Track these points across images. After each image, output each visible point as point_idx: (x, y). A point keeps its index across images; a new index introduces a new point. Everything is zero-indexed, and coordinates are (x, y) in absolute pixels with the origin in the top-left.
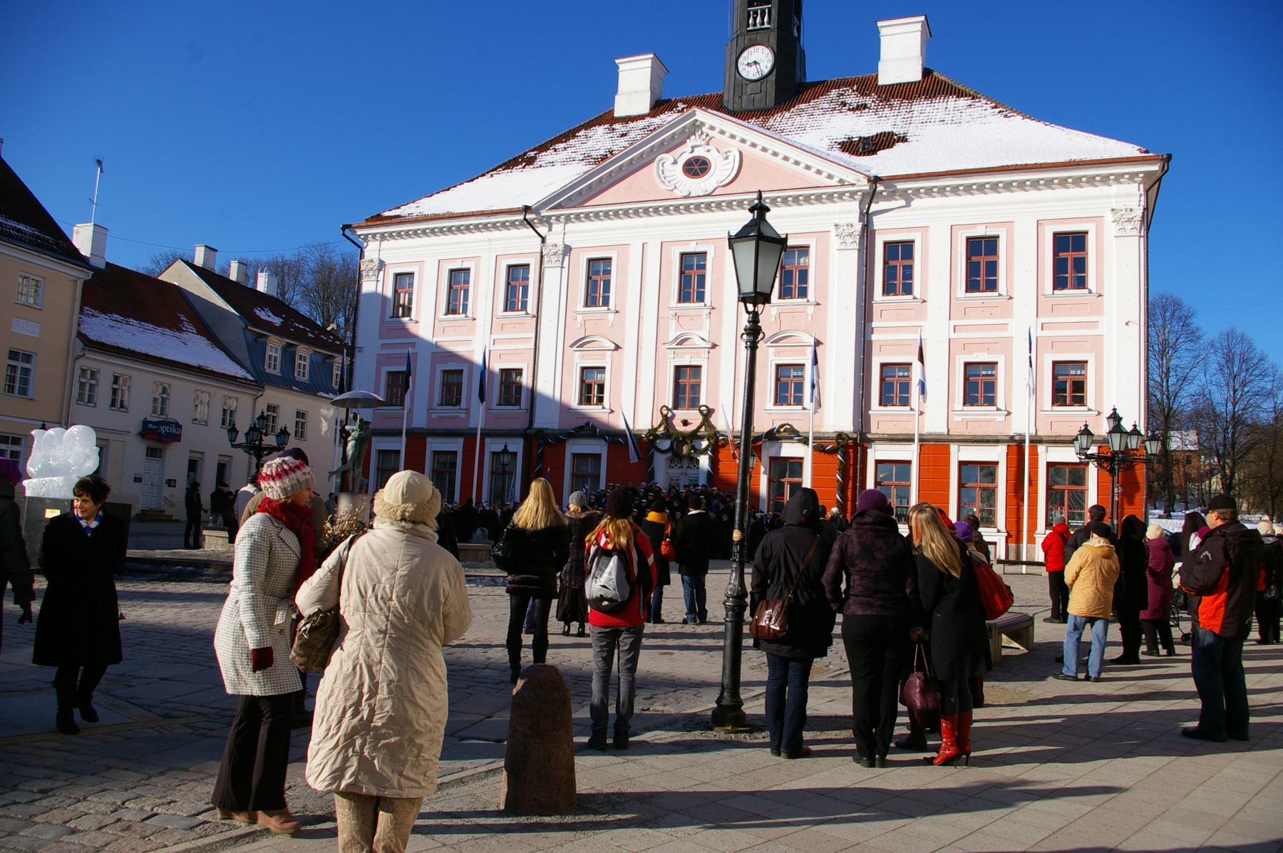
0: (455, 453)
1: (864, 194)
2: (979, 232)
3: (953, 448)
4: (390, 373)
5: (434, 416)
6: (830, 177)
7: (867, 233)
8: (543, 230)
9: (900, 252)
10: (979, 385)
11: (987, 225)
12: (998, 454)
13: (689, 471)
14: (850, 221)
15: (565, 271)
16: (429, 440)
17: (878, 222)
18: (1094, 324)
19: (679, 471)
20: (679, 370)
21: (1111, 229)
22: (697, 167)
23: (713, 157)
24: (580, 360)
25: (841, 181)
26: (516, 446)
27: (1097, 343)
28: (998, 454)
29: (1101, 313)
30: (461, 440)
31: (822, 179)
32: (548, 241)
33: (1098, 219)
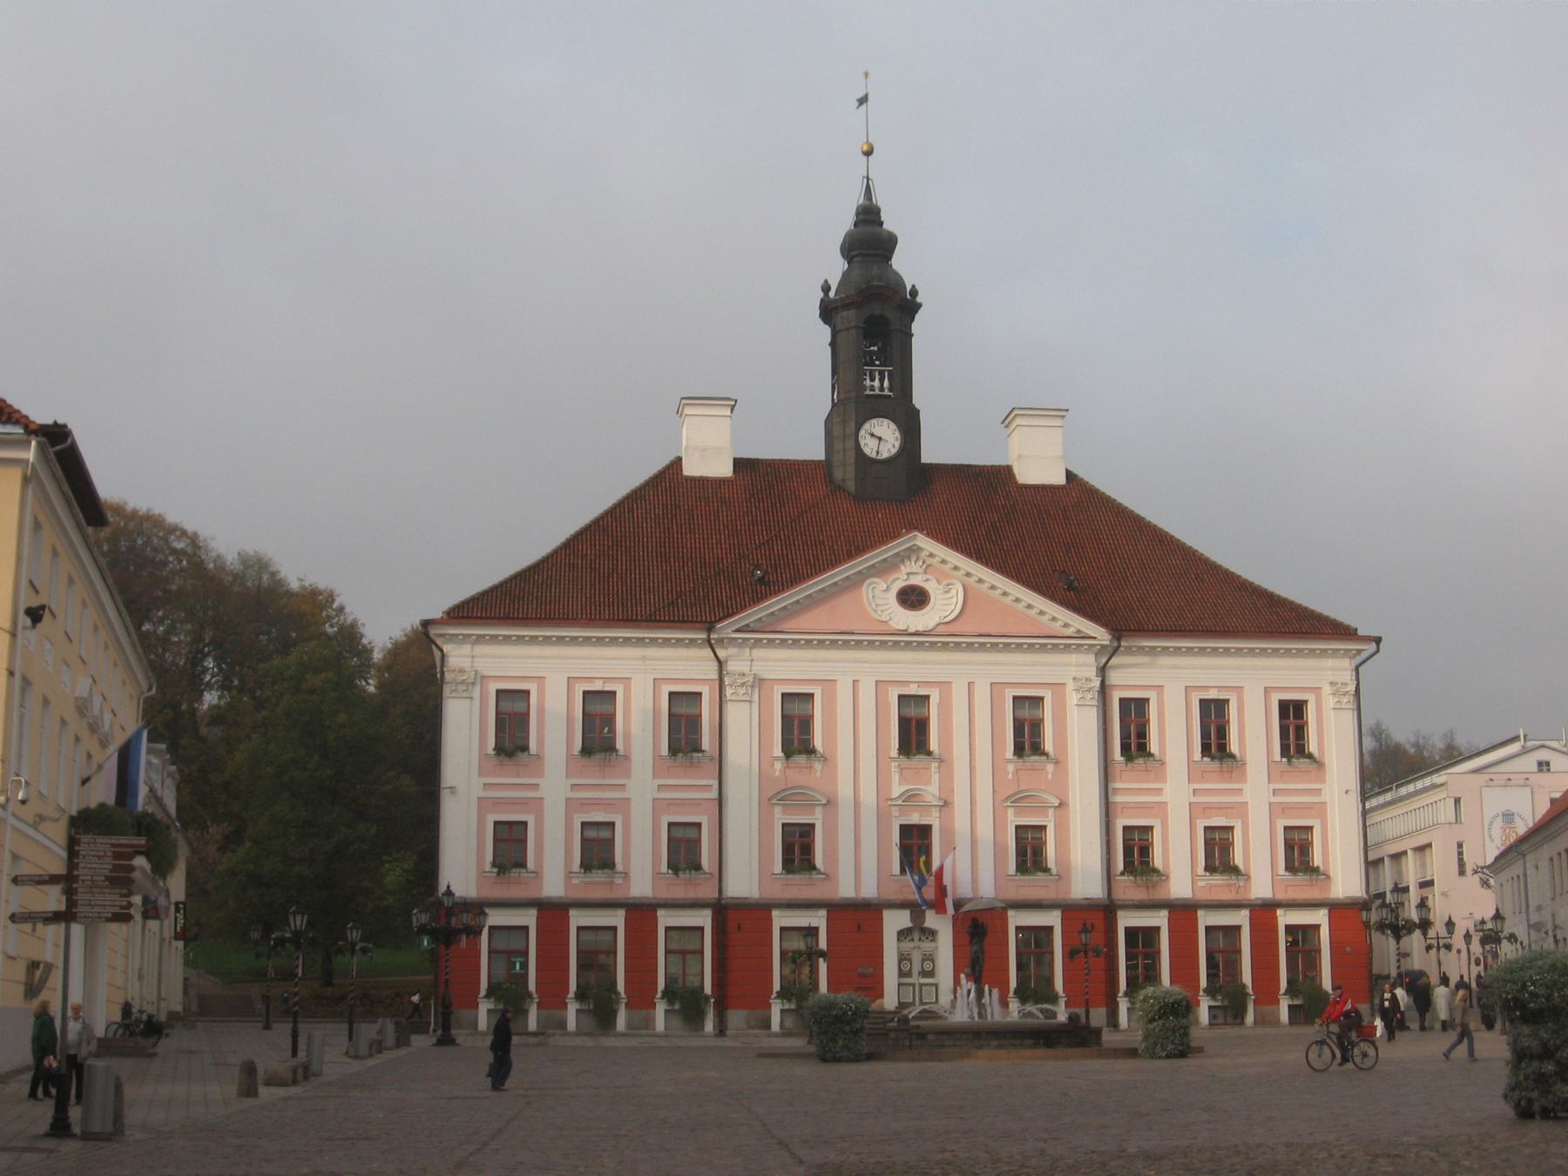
0: (614, 929)
1: (1103, 647)
2: (1213, 695)
3: (1200, 913)
4: (496, 823)
5: (575, 881)
6: (1066, 625)
7: (1104, 690)
8: (721, 653)
9: (1135, 710)
10: (1218, 851)
12: (1241, 918)
14: (1088, 675)
15: (755, 706)
16: (573, 913)
17: (1114, 678)
18: (1318, 792)
19: (911, 945)
20: (906, 830)
21: (1329, 702)
22: (913, 598)
23: (927, 586)
24: (780, 817)
25: (1079, 631)
26: (704, 919)
27: (1320, 810)
28: (1241, 918)
29: (1323, 781)
30: (621, 913)
31: (1057, 628)
32: (732, 666)
33: (1317, 690)
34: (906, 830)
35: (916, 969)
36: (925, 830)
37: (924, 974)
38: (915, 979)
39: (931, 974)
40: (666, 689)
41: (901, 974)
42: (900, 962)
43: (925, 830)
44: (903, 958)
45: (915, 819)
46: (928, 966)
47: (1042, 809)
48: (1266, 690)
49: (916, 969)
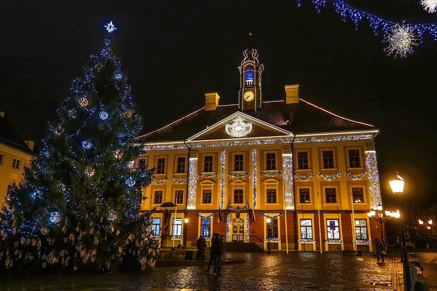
11: (329, 148)
13: (240, 223)
19: (237, 223)
34: (236, 191)
35: (238, 230)
36: (241, 191)
37: (241, 232)
38: (238, 233)
39: (243, 232)
40: (177, 157)
41: (234, 232)
42: (234, 228)
43: (241, 191)
44: (234, 227)
45: (238, 188)
46: (242, 230)
47: (275, 185)
48: (344, 147)
49: (238, 230)
